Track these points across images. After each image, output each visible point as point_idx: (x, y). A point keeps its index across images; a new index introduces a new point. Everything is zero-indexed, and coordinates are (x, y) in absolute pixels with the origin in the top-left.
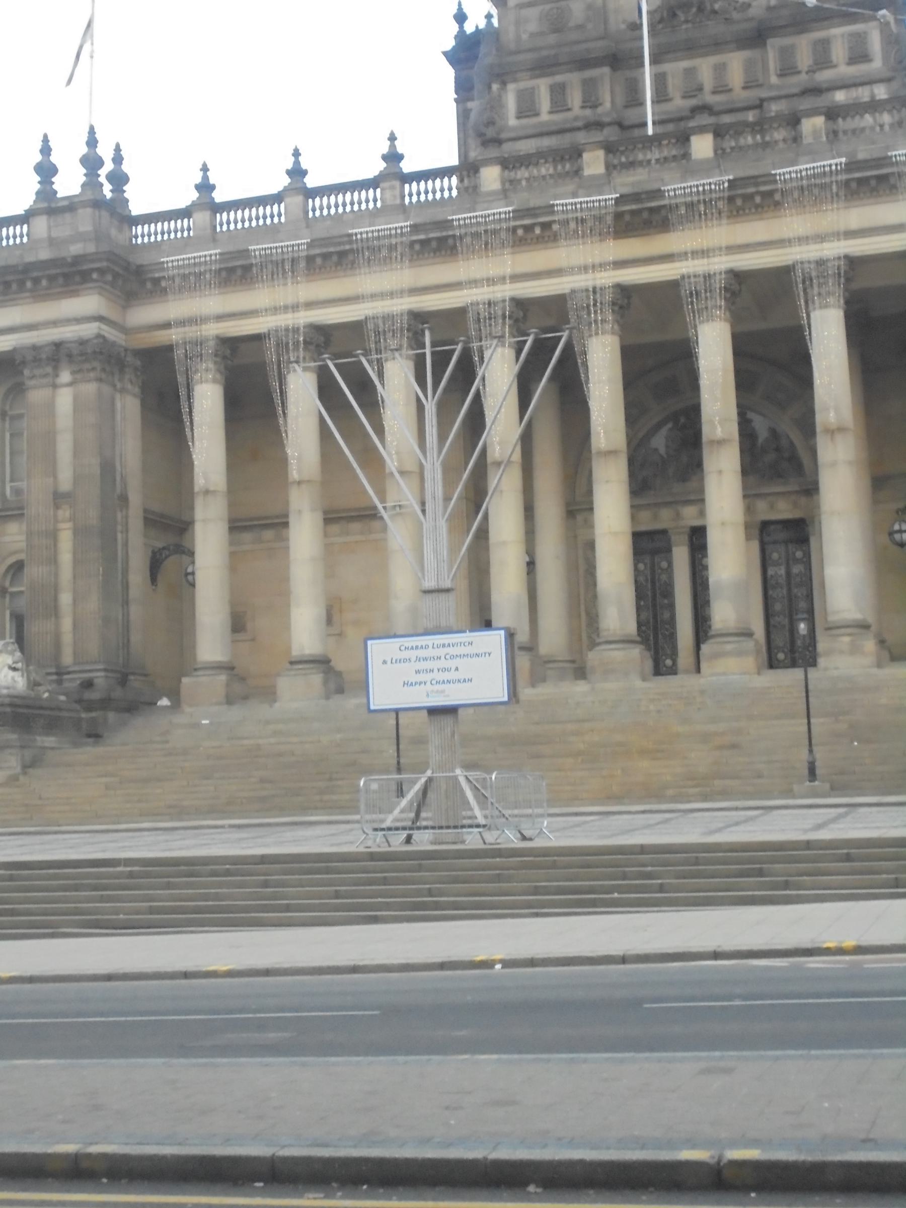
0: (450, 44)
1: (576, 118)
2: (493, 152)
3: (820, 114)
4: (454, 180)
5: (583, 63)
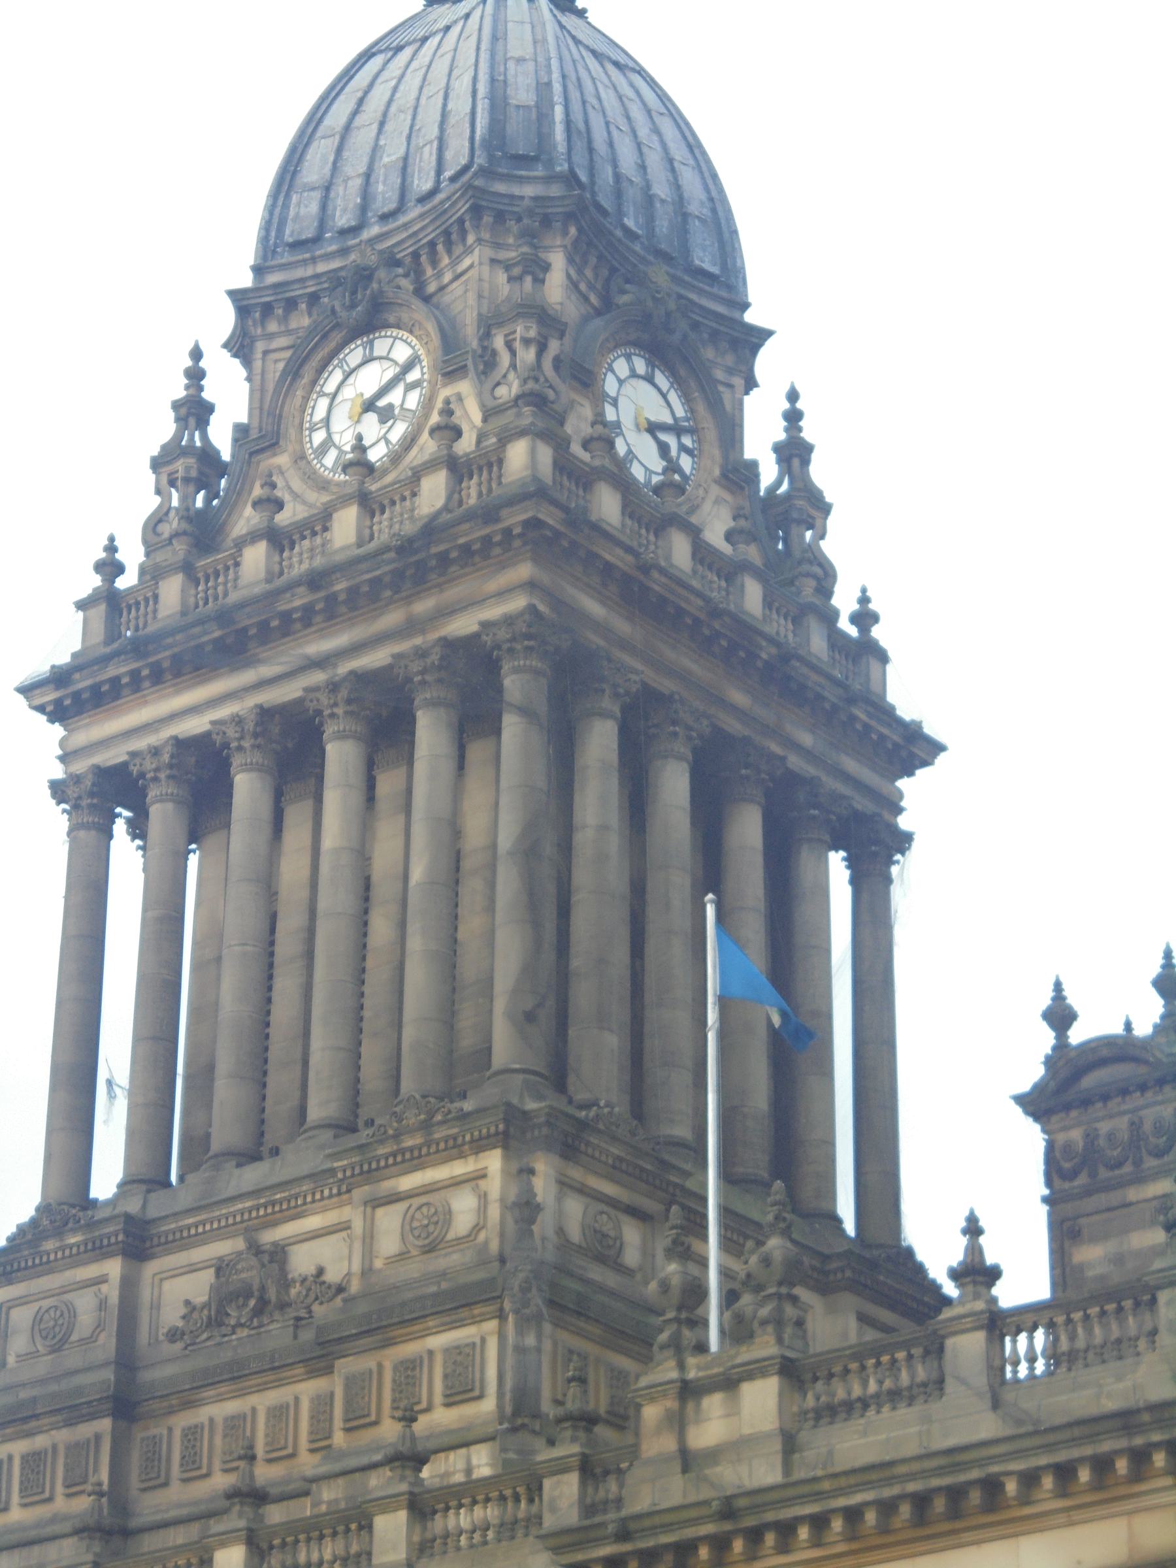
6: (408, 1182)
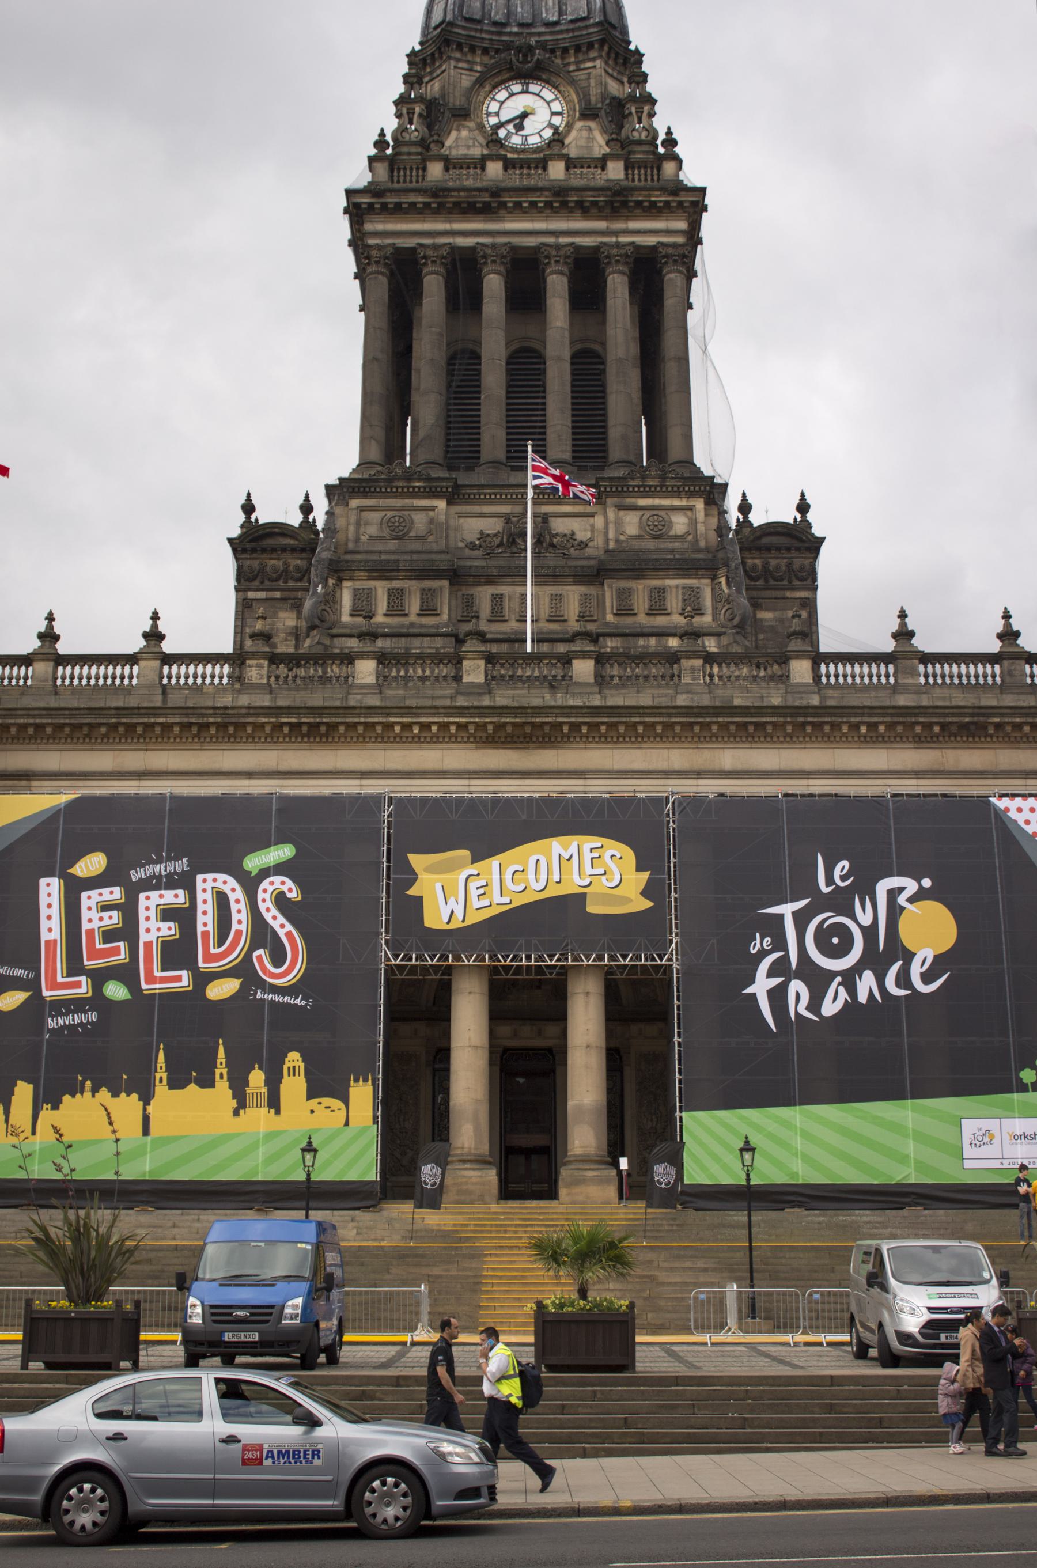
0: (236, 532)
1: (412, 625)
2: (369, 647)
3: (698, 658)
4: (226, 669)
5: (422, 573)
6: (642, 502)
